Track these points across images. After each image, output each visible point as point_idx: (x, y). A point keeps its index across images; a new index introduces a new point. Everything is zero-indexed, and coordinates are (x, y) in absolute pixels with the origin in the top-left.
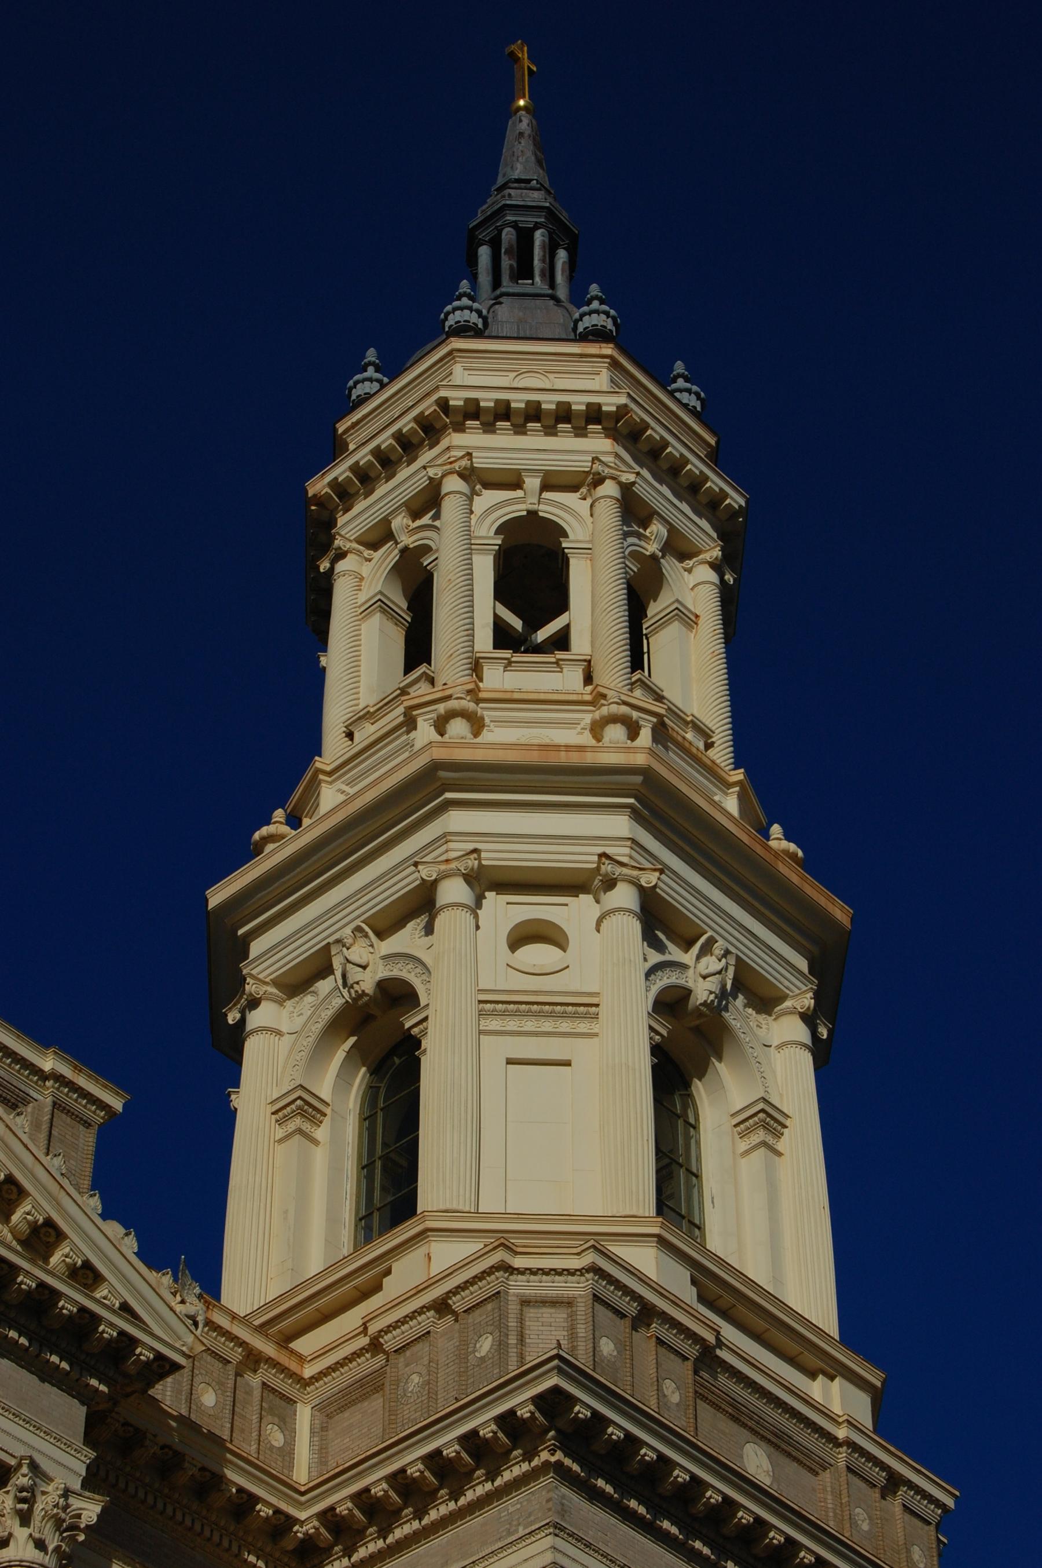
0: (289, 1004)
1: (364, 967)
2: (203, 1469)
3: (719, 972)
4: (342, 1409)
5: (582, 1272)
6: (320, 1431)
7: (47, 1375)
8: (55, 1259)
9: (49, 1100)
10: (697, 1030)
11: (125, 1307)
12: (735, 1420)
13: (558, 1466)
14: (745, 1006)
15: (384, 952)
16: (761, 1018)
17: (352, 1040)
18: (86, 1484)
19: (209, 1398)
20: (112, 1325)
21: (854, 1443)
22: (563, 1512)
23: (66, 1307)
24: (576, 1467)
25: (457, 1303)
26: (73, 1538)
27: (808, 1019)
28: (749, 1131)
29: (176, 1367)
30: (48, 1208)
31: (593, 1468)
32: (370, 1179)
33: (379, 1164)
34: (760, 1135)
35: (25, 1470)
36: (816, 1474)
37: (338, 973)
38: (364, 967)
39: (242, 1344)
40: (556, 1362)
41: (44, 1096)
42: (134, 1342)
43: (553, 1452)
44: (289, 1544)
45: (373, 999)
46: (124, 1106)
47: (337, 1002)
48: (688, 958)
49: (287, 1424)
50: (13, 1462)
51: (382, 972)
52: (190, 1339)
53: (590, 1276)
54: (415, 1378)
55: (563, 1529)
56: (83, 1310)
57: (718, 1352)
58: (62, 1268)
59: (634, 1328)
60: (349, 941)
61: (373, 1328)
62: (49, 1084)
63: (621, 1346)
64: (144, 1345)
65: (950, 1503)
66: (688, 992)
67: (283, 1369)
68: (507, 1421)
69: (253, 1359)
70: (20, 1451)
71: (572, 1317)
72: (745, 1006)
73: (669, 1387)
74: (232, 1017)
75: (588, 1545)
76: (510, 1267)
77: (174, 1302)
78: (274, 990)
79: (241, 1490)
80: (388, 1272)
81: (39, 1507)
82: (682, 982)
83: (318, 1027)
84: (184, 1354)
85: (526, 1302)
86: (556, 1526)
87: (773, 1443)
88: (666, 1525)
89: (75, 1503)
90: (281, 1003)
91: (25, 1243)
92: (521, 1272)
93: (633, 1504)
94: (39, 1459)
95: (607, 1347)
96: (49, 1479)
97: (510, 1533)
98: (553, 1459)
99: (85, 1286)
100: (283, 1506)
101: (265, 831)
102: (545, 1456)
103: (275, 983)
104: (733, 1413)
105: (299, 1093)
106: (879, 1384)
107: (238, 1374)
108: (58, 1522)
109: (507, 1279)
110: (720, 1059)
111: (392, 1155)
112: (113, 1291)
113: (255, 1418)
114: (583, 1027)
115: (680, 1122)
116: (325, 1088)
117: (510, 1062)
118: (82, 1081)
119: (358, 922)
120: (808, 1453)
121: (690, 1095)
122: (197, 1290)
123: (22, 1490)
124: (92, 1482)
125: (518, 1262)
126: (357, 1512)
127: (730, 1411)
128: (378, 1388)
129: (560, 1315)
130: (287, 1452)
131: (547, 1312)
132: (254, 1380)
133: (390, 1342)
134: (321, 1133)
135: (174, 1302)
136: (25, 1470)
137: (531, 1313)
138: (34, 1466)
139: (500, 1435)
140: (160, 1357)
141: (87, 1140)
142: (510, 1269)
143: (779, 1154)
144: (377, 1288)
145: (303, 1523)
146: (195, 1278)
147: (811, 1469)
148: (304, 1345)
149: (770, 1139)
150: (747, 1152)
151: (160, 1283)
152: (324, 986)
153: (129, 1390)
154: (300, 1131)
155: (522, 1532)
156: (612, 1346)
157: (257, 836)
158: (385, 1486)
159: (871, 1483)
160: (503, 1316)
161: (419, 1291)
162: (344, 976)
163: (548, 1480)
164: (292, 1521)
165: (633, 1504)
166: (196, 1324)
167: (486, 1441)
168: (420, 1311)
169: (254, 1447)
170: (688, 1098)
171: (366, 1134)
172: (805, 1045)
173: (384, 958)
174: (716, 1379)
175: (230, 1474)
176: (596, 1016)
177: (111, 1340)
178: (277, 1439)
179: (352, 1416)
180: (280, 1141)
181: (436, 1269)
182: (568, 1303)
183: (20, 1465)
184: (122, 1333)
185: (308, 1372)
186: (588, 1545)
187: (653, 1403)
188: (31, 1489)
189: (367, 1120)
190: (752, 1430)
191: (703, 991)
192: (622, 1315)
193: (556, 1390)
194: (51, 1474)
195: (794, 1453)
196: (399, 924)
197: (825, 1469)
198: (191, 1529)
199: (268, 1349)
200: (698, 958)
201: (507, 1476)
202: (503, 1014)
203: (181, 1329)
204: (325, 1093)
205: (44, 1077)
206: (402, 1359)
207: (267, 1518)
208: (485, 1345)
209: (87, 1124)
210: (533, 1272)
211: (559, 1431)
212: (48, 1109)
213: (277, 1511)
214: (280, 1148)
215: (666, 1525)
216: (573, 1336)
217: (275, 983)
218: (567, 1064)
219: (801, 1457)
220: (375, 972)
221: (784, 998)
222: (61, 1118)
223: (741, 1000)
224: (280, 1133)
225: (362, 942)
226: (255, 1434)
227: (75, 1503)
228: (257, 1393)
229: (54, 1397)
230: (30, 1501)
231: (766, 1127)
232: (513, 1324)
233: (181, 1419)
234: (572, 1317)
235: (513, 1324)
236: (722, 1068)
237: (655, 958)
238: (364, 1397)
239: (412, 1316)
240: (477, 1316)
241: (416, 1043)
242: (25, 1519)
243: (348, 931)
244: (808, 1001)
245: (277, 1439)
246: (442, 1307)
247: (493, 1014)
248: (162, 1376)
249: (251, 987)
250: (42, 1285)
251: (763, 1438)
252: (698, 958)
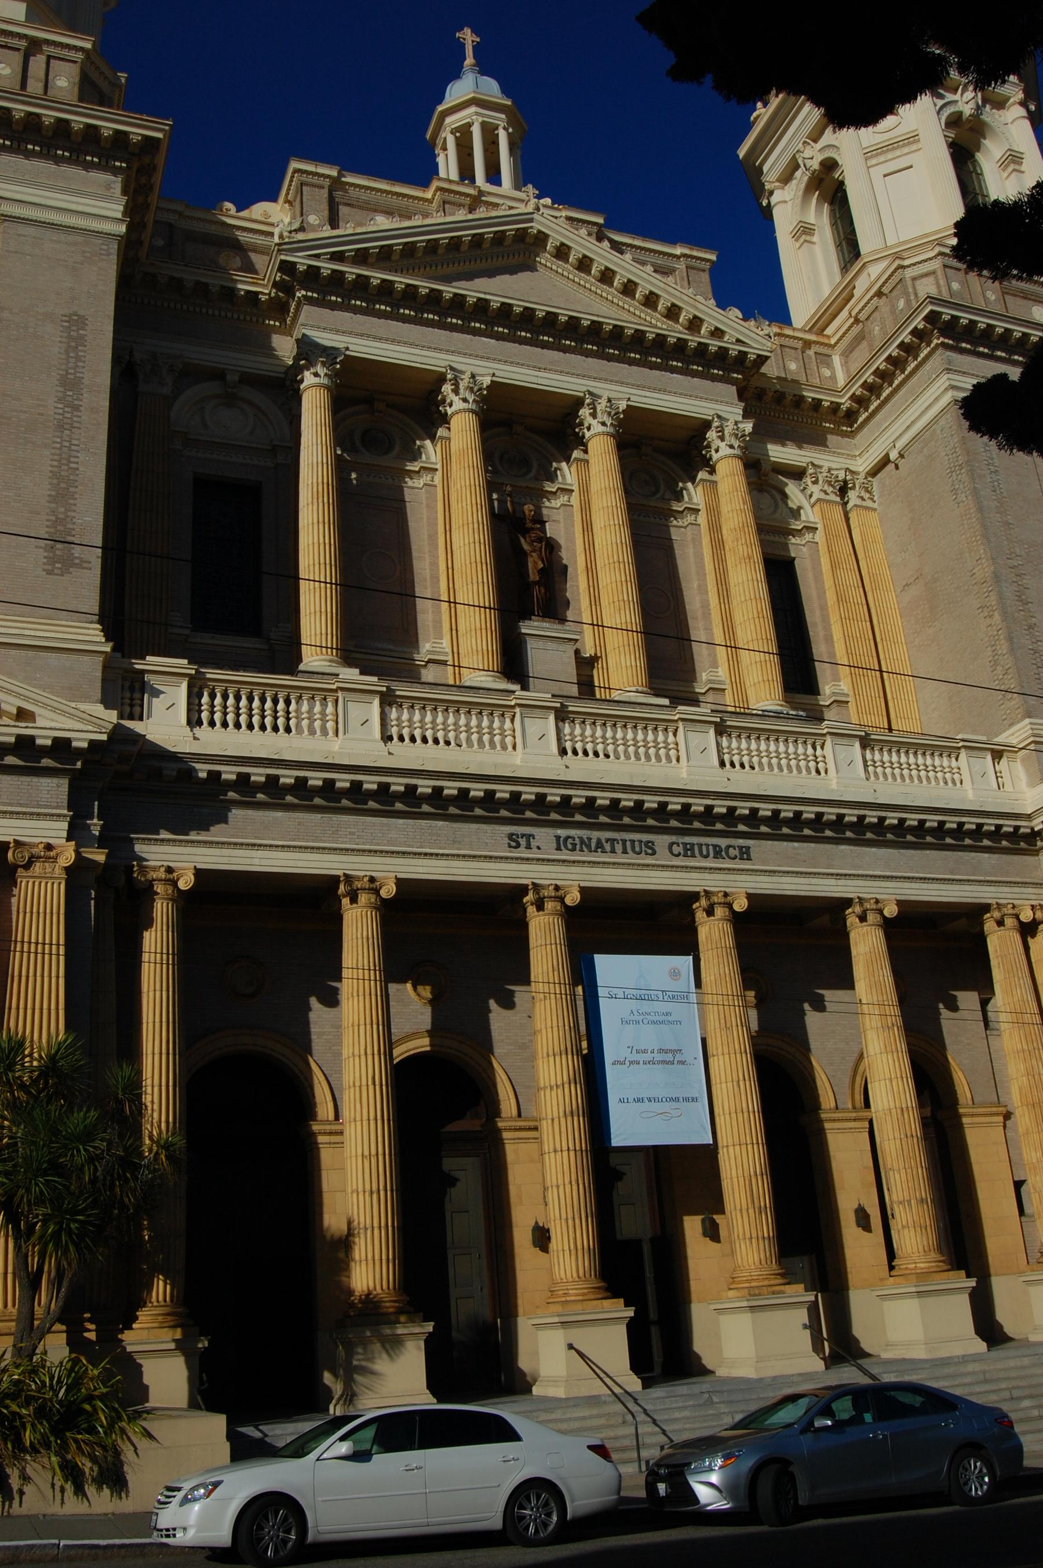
0: (786, 187)
1: (812, 158)
2: (795, 395)
3: (974, 98)
4: (851, 352)
5: (935, 257)
6: (845, 364)
7: (714, 379)
8: (702, 332)
9: (684, 266)
10: (971, 129)
11: (738, 341)
12: (1024, 298)
13: (943, 344)
14: (991, 109)
15: (818, 148)
16: (1001, 112)
17: (817, 193)
18: (745, 416)
19: (793, 366)
20: (734, 350)
22: (949, 363)
23: (713, 349)
24: (951, 342)
25: (885, 290)
26: (744, 440)
27: (1023, 104)
28: (1007, 166)
29: (767, 358)
30: (692, 311)
31: (958, 339)
32: (842, 251)
33: (844, 243)
34: (1012, 167)
35: (716, 419)
37: (802, 166)
38: (812, 158)
39: (801, 339)
40: (928, 300)
41: (681, 266)
42: (746, 353)
43: (938, 339)
44: (841, 414)
45: (820, 171)
46: (717, 257)
47: (806, 178)
48: (957, 97)
49: (830, 366)
50: (710, 418)
51: (820, 157)
52: (769, 344)
53: (939, 257)
54: (877, 328)
55: (950, 370)
56: (720, 348)
58: (707, 333)
59: (966, 273)
60: (802, 149)
61: (854, 314)
62: (682, 259)
63: (961, 283)
64: (751, 353)
66: (960, 114)
67: (822, 344)
68: (915, 332)
69: (808, 344)
70: (712, 412)
71: (936, 279)
72: (991, 109)
73: (989, 294)
74: (765, 203)
75: (964, 373)
77: (758, 331)
78: (777, 184)
79: (813, 399)
80: (854, 288)
81: (726, 432)
82: (957, 109)
83: (801, 193)
84: (768, 351)
85: (914, 279)
86: (947, 369)
88: (999, 353)
89: (741, 426)
90: (783, 188)
91: (689, 329)
92: (909, 266)
93: (981, 349)
94: (720, 413)
95: (955, 286)
96: (727, 420)
97: (929, 379)
98: (939, 342)
99: (720, 338)
100: (834, 399)
101: (755, 115)
102: (935, 341)
103: (778, 180)
105: (801, 224)
107: (803, 352)
108: (736, 435)
110: (985, 138)
111: (849, 236)
112: (731, 336)
113: (815, 368)
114: (914, 147)
115: (974, 174)
116: (811, 218)
117: (885, 176)
118: (695, 253)
119: (804, 139)
121: (976, 161)
122: (767, 323)
123: (717, 428)
124: (746, 415)
125: (906, 263)
126: (864, 392)
128: (863, 338)
129: (931, 279)
130: (833, 377)
131: (924, 280)
132: (811, 353)
133: (862, 317)
134: (815, 239)
135: (758, 331)
136: (716, 419)
137: (918, 283)
138: (719, 417)
139: (914, 339)
140: (759, 356)
141: (706, 277)
142: (903, 267)
143: (1023, 172)
144: (853, 296)
145: (844, 404)
146: (765, 319)
148: (828, 331)
149: (1017, 167)
150: (1008, 176)
151: (750, 326)
152: (798, 174)
153: (752, 373)
154: (806, 241)
155: (934, 376)
156: (957, 284)
157: (752, 118)
158: (872, 377)
160: (906, 288)
161: (868, 291)
162: (805, 166)
163: (940, 351)
164: (839, 405)
165: (981, 349)
166: (770, 337)
167: (909, 344)
168: (871, 299)
169: (818, 380)
170: (975, 163)
171: (835, 232)
172: (1024, 117)
173: (819, 151)
175: (805, 394)
176: (919, 140)
177: (736, 356)
178: (827, 373)
179: (856, 354)
180: (799, 248)
181: (873, 278)
182: (934, 273)
183: (713, 418)
184: (740, 351)
185: (833, 341)
186: (964, 373)
187: (983, 302)
188: (721, 426)
189: (834, 225)
191: (967, 110)
192: (959, 270)
193: (932, 312)
194: (727, 417)
196: (822, 133)
198: (798, 421)
199: (812, 337)
200: (962, 95)
201: (922, 355)
202: (877, 155)
203: (764, 341)
204: (812, 220)
205: (678, 257)
206: (869, 322)
207: (828, 406)
208: (901, 303)
209: (704, 271)
210: (914, 264)
211: (939, 329)
212: (685, 270)
213: (832, 402)
214: (800, 252)
215: (999, 353)
216: (938, 286)
217: (778, 180)
218: (911, 167)
220: (817, 159)
221: (1009, 98)
222: (692, 272)
223: (988, 107)
224: (798, 245)
225: (808, 147)
226: (817, 374)
227: (741, 426)
228: (813, 357)
229: (720, 386)
230: (722, 431)
231: (1014, 162)
232: (911, 290)
233: (778, 378)
234: (936, 279)
235: (911, 290)
236: (987, 143)
237: (940, 103)
238: (859, 344)
239: (868, 302)
240: (895, 293)
241: (842, 183)
242: (722, 438)
243: (800, 145)
244: (1021, 96)
245: (827, 373)
246: (879, 294)
247: (872, 157)
248: (763, 363)
249: (767, 187)
250: (700, 343)
252: (962, 95)
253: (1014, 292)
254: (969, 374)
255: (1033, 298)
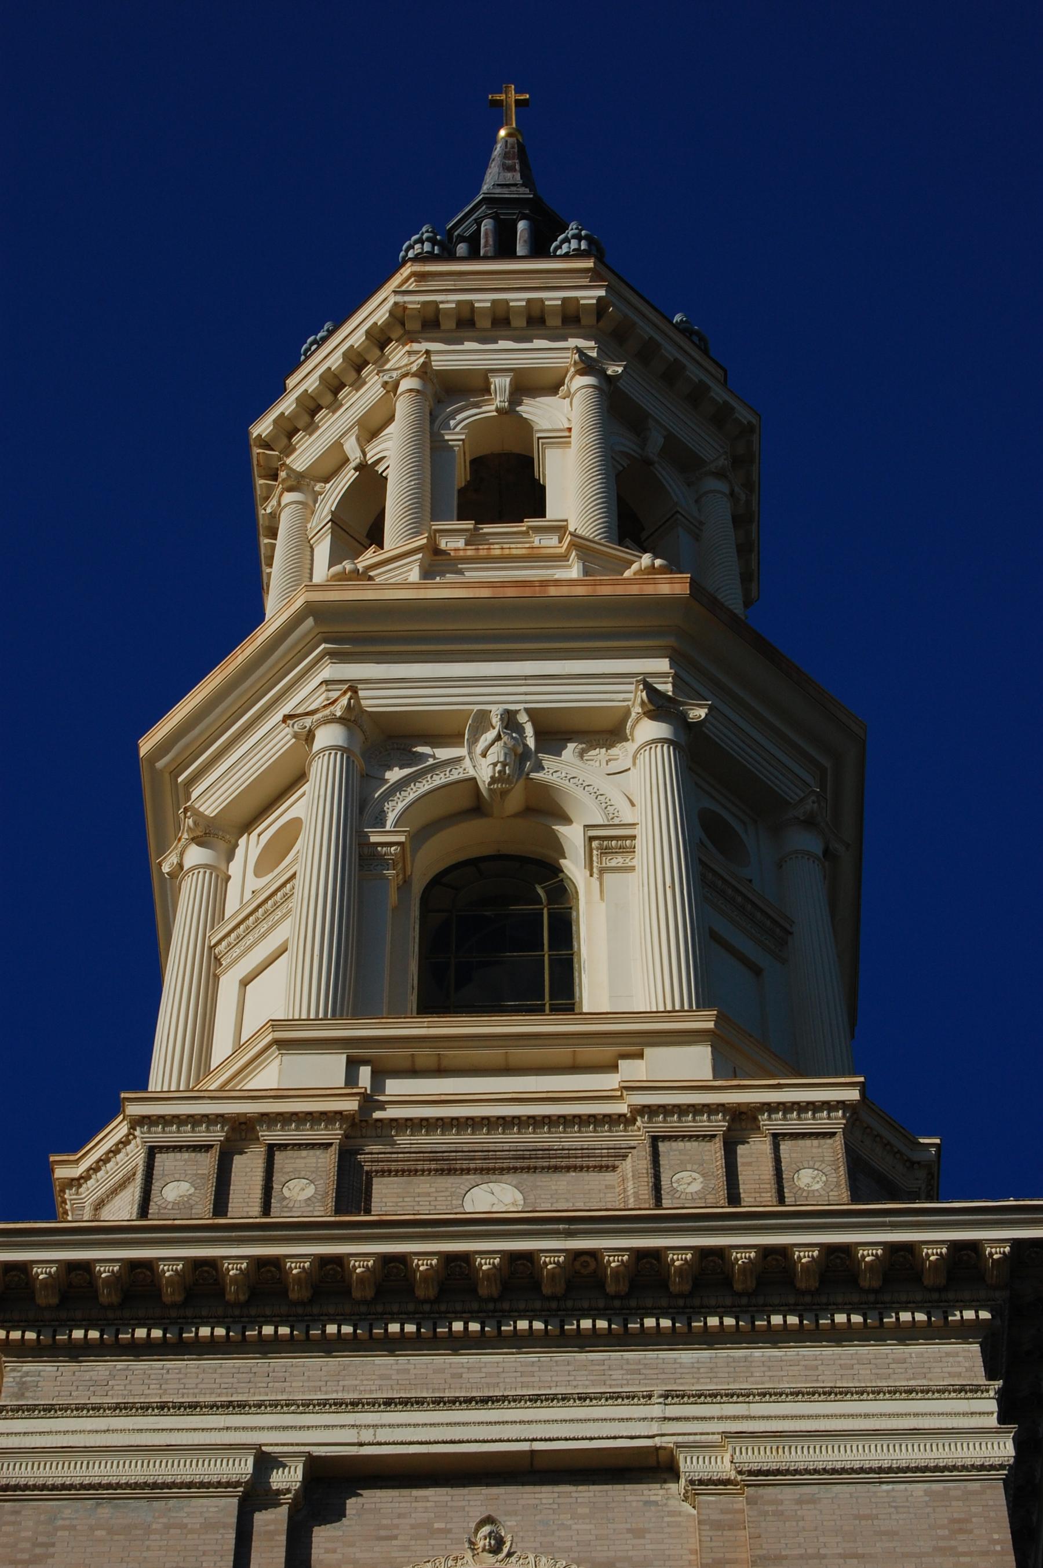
12: (441, 1172)
21: (644, 1106)
36: (614, 1168)
57: (378, 1115)
65: (853, 1095)
76: (73, 1179)
87: (522, 1169)
92: (85, 1177)
104: (438, 1167)
106: (711, 1025)
109: (77, 1194)
120: (587, 1153)
127: (433, 1167)
147: (601, 1167)
159: (705, 1136)
174: (394, 1144)
190: (481, 1171)
195: (564, 1163)
197: (625, 1157)
210: (95, 1169)
219: (572, 1162)
251: (502, 1171)
253: (400, 1166)
254: (65, 1408)
255: (479, 1164)
